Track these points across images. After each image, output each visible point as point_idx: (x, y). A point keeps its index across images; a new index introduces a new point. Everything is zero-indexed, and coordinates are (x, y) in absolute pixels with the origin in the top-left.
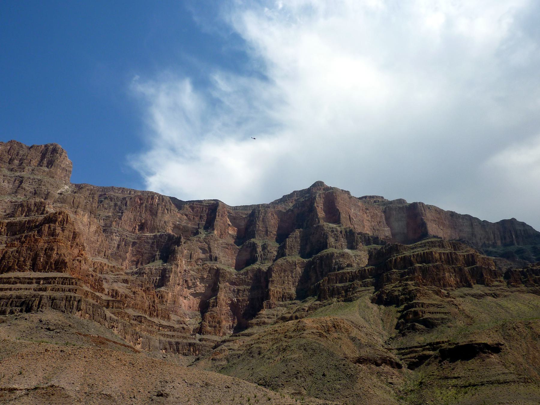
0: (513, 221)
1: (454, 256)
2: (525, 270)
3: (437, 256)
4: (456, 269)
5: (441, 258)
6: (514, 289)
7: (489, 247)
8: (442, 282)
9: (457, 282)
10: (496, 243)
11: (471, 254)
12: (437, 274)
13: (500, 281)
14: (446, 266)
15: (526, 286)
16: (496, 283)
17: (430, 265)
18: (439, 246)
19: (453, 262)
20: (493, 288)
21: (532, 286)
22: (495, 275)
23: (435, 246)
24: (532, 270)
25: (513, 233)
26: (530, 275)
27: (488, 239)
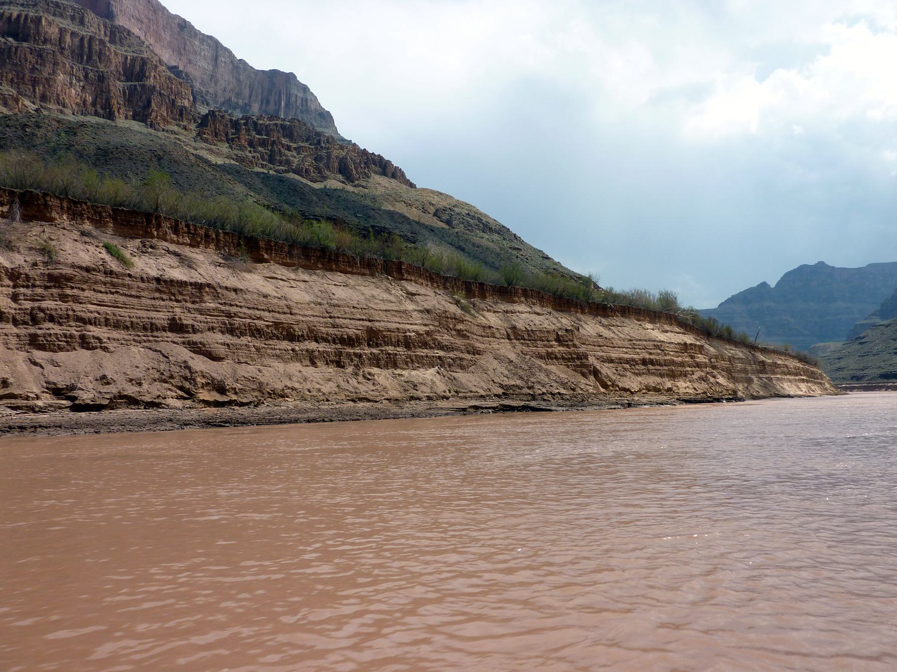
0: (290, 78)
1: (96, 47)
2: (243, 122)
3: (53, 32)
4: (91, 75)
5: (61, 40)
6: (204, 145)
7: (235, 108)
8: (39, 90)
9: (85, 102)
10: (250, 106)
11: (142, 59)
12: (33, 69)
13: (185, 128)
14: (68, 63)
15: (231, 147)
16: (176, 128)
17: (25, 44)
18: (73, 18)
19: (90, 58)
20: (160, 134)
21: (242, 148)
22: (181, 114)
23: (61, 16)
24: (255, 124)
25: (284, 97)
26: (248, 130)
27: (238, 95)
